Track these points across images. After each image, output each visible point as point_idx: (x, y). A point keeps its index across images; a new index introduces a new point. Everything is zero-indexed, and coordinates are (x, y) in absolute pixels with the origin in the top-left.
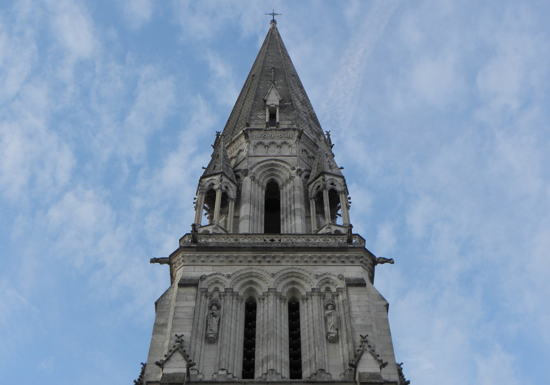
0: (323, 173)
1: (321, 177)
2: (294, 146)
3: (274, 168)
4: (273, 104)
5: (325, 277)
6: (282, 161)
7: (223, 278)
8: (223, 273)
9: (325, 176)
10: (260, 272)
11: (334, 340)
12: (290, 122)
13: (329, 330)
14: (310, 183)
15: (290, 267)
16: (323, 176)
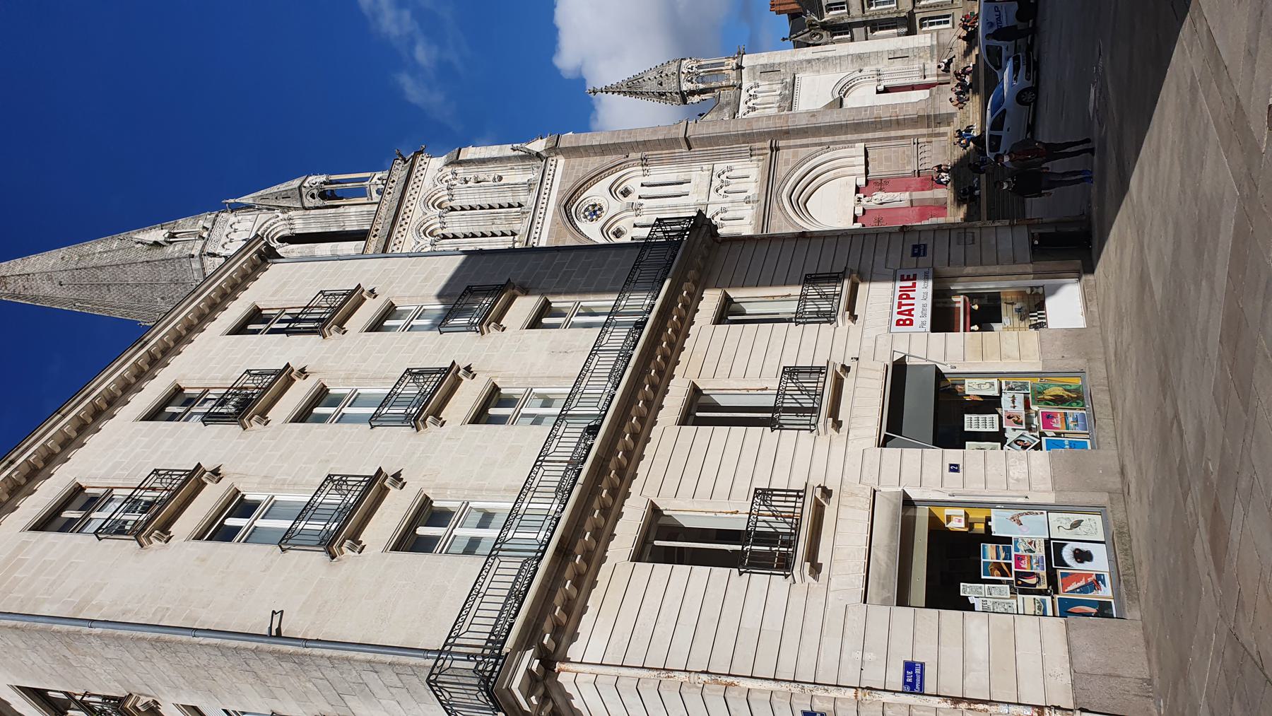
0: (300, 188)
1: (303, 189)
2: (240, 218)
3: (266, 233)
4: (164, 235)
5: (436, 181)
6: (263, 225)
7: (417, 247)
8: (413, 246)
9: (305, 185)
10: (417, 223)
11: (500, 178)
12: (200, 221)
13: (491, 179)
14: (302, 204)
15: (418, 202)
16: (305, 187)
